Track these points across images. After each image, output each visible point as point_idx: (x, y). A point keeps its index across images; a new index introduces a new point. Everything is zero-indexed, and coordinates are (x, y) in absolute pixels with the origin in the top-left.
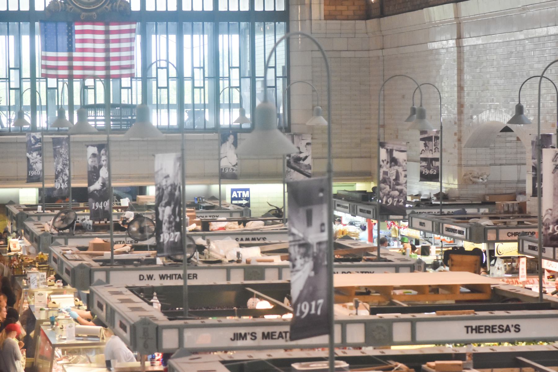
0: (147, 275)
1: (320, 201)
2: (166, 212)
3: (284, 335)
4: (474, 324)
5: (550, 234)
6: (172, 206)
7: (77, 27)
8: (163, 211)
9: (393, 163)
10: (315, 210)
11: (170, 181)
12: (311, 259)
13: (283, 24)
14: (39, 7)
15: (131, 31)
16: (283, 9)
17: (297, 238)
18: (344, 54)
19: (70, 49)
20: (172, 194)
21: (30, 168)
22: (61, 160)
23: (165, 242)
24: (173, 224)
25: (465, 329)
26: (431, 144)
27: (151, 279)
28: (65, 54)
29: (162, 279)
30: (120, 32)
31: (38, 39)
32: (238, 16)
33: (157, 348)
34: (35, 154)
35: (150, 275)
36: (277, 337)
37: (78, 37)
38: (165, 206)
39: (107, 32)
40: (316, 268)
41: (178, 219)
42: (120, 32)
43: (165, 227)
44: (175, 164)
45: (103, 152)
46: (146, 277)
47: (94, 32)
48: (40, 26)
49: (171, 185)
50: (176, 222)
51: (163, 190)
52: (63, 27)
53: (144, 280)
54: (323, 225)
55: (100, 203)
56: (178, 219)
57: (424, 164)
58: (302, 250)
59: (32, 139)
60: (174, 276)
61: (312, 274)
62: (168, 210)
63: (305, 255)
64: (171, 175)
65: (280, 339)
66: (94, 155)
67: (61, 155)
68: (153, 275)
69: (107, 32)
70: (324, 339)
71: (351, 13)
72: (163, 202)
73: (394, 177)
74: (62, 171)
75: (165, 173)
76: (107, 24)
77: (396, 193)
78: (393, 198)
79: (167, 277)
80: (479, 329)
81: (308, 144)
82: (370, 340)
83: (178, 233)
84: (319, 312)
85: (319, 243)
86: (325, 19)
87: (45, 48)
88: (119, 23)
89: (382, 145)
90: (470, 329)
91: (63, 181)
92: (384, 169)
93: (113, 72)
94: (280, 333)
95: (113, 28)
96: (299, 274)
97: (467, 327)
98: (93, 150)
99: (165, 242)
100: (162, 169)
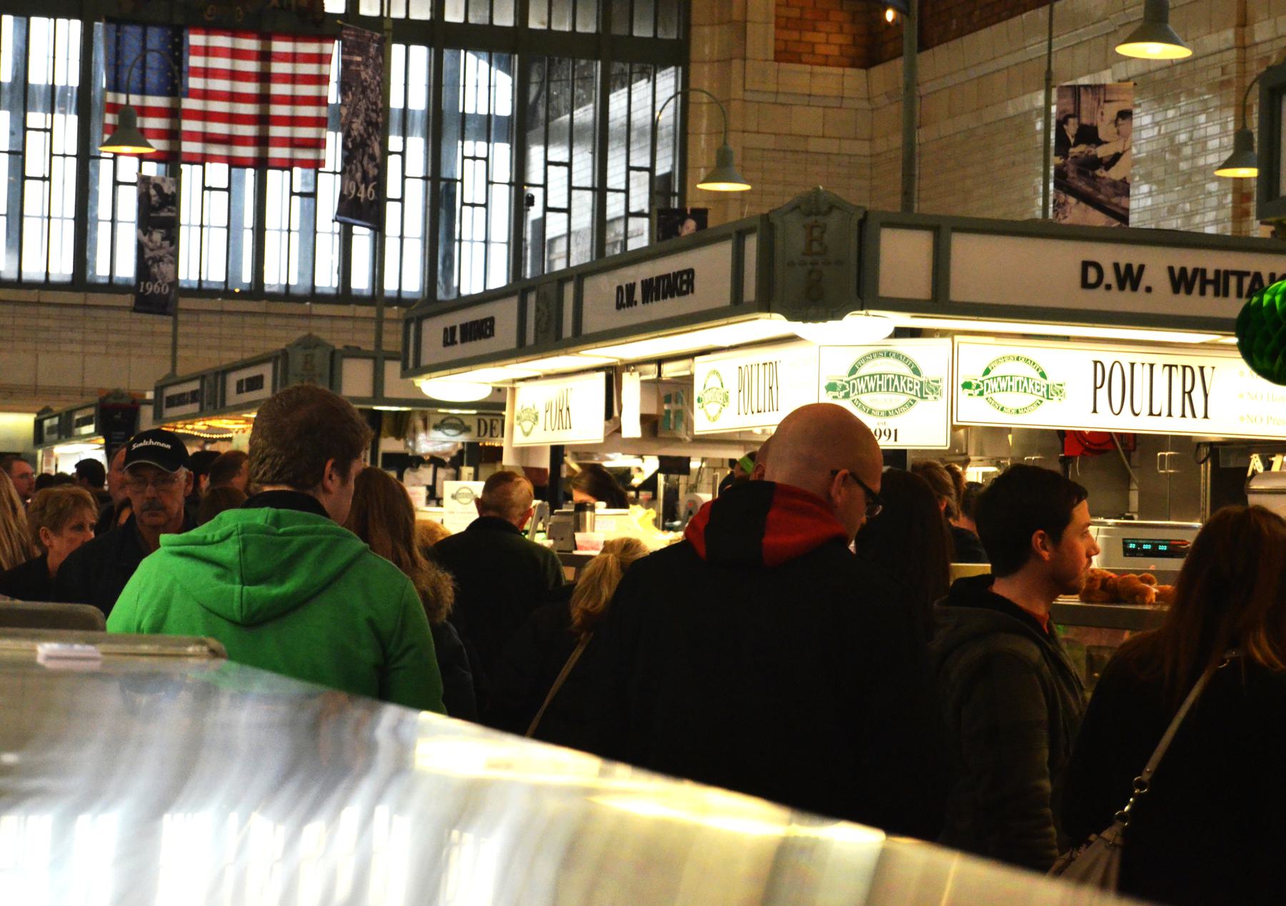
0: (1116, 266)
7: (196, 40)
18: (814, 145)
19: (174, 88)
22: (362, 105)
27: (1135, 288)
29: (1182, 290)
34: (157, 236)
35: (1129, 267)
39: (265, 56)
42: (294, 58)
46: (1110, 277)
47: (235, 54)
48: (107, 31)
53: (1101, 290)
59: (153, 192)
60: (1233, 281)
67: (364, 92)
68: (1142, 268)
71: (833, 50)
76: (266, 37)
79: (1205, 282)
86: (776, 60)
88: (294, 37)
91: (365, 179)
93: (276, 152)
95: (280, 46)
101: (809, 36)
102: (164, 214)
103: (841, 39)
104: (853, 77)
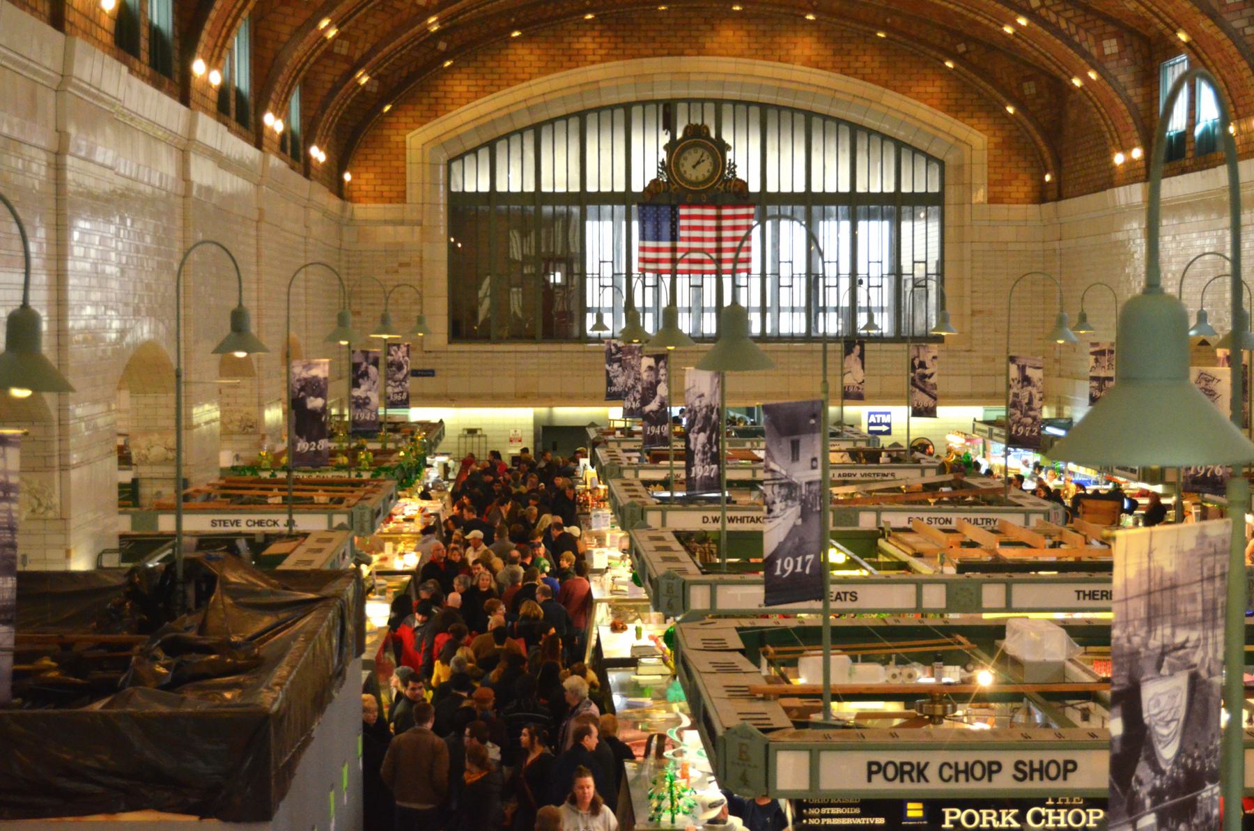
1: (813, 430)
2: (699, 440)
3: (843, 596)
4: (1088, 588)
5: (1191, 476)
6: (708, 432)
7: (683, 212)
8: (696, 439)
9: (1025, 383)
10: (804, 440)
11: (705, 402)
12: (798, 502)
13: (937, 208)
14: (637, 187)
15: (748, 216)
16: (937, 190)
17: (778, 476)
18: (1011, 247)
19: (674, 238)
20: (707, 418)
21: (610, 383)
22: (632, 373)
23: (698, 477)
24: (709, 455)
25: (1076, 594)
26: (1104, 360)
28: (666, 244)
30: (735, 217)
31: (635, 225)
32: (881, 198)
33: (684, 608)
34: (616, 366)
36: (833, 598)
37: (683, 223)
38: (698, 433)
39: (719, 218)
40: (804, 515)
41: (715, 449)
42: (735, 217)
43: (697, 458)
44: (712, 381)
45: (662, 364)
46: (710, 520)
47: (703, 217)
49: (707, 407)
50: (712, 452)
51: (696, 412)
52: (666, 211)
54: (814, 459)
55: (656, 427)
56: (715, 449)
57: (1095, 384)
58: (784, 491)
59: (613, 347)
61: (799, 522)
62: (702, 437)
63: (786, 498)
64: (706, 394)
65: (838, 601)
66: (650, 368)
67: (633, 368)
69: (719, 218)
70: (818, 605)
72: (696, 428)
73: (1026, 401)
74: (634, 387)
75: (698, 391)
76: (719, 207)
77: (1029, 420)
78: (1025, 426)
80: (1094, 595)
81: (934, 358)
82: (953, 603)
83: (715, 467)
84: (807, 571)
85: (809, 483)
87: (643, 237)
88: (735, 206)
89: (1012, 359)
90: (1081, 595)
91: (635, 400)
92: (1015, 390)
94: (839, 594)
96: (777, 521)
97: (1078, 592)
98: (647, 362)
99: (698, 477)
100: (694, 386)
101: (1008, 189)
102: (619, 356)
103: (1026, 189)
104: (1034, 209)
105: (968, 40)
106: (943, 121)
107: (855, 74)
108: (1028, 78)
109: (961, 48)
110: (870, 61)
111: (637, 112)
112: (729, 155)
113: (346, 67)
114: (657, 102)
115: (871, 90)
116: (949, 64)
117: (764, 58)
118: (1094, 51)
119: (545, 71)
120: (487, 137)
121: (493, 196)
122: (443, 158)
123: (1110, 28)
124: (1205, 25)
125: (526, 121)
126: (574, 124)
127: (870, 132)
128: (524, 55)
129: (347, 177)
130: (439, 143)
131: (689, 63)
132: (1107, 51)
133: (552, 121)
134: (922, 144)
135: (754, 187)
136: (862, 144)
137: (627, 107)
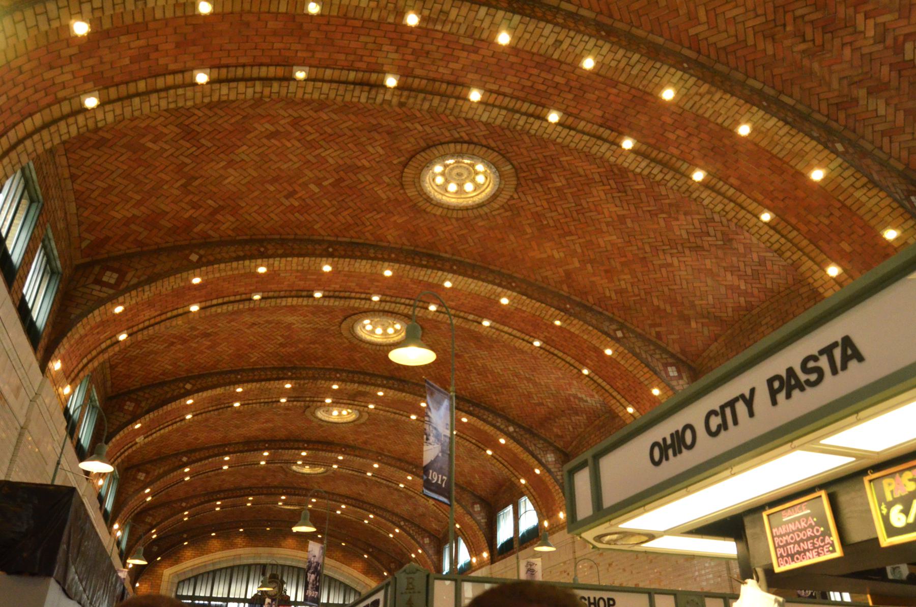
14: (249, 596)
66: (269, 603)
105: (373, 547)
106: (362, 577)
107: (333, 558)
108: (392, 562)
109: (371, 550)
110: (338, 554)
111: (253, 568)
112: (285, 586)
113: (149, 527)
114: (260, 564)
115: (338, 564)
116: (366, 556)
117: (302, 550)
118: (421, 542)
119: (223, 549)
120: (195, 573)
121: (193, 598)
122: (176, 581)
123: (426, 535)
124: (467, 519)
125: (211, 568)
126: (229, 571)
127: (336, 580)
128: (215, 543)
129: (137, 585)
130: (177, 574)
131: (275, 550)
132: (426, 542)
133: (221, 570)
134: (353, 585)
135: (292, 599)
136: (333, 585)
137: (249, 566)
